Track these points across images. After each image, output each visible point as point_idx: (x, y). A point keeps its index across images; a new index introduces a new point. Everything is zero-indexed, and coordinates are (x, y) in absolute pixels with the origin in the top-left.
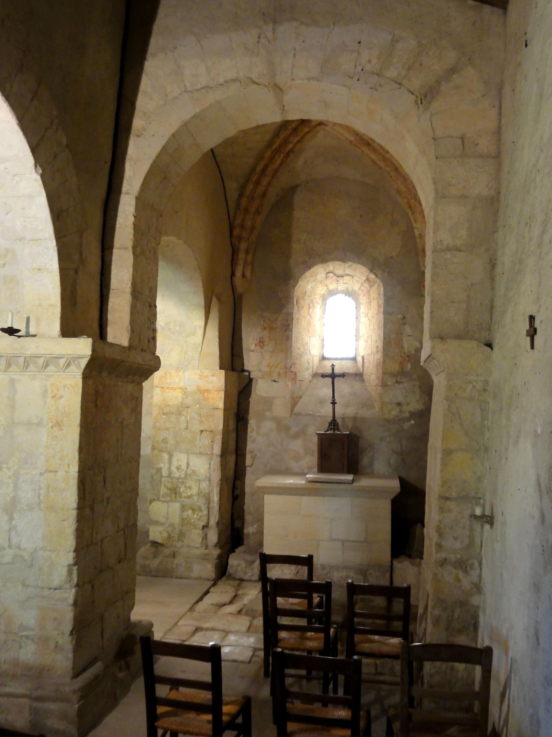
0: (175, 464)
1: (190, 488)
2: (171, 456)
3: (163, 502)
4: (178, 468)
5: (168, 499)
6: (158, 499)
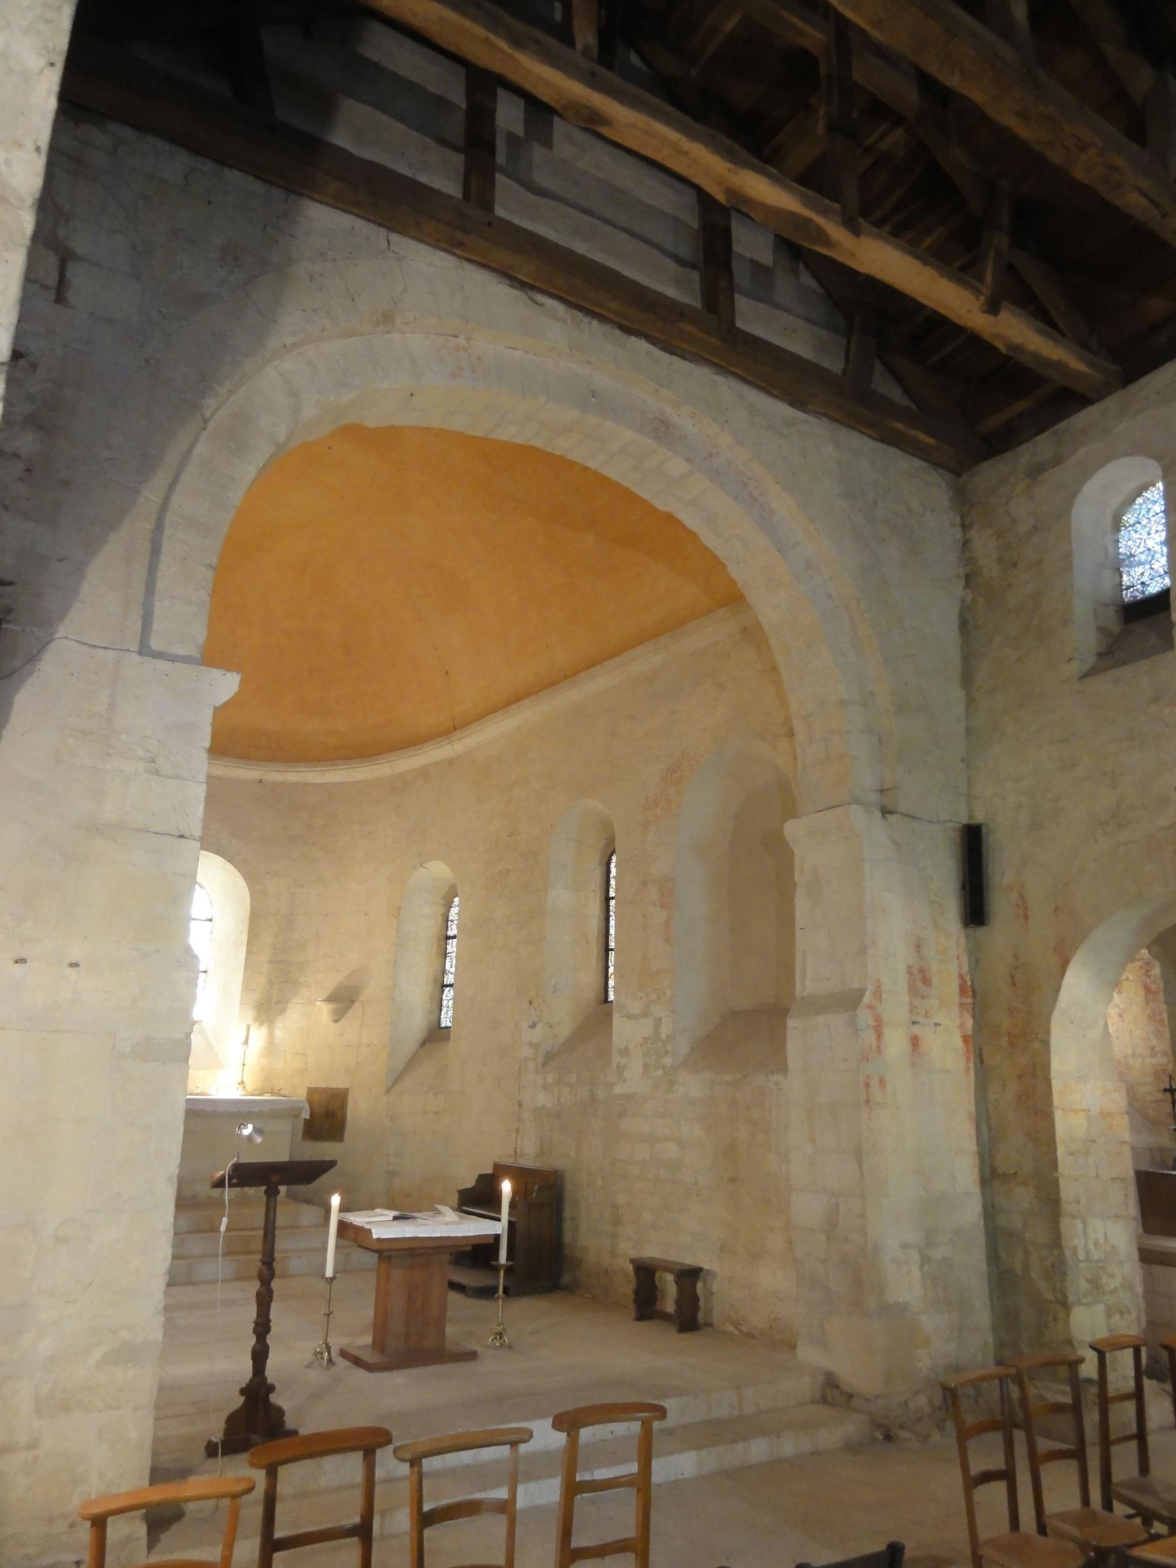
1: (1112, 1276)
2: (1085, 1224)
3: (1084, 1305)
4: (1096, 1244)
5: (1090, 1299)
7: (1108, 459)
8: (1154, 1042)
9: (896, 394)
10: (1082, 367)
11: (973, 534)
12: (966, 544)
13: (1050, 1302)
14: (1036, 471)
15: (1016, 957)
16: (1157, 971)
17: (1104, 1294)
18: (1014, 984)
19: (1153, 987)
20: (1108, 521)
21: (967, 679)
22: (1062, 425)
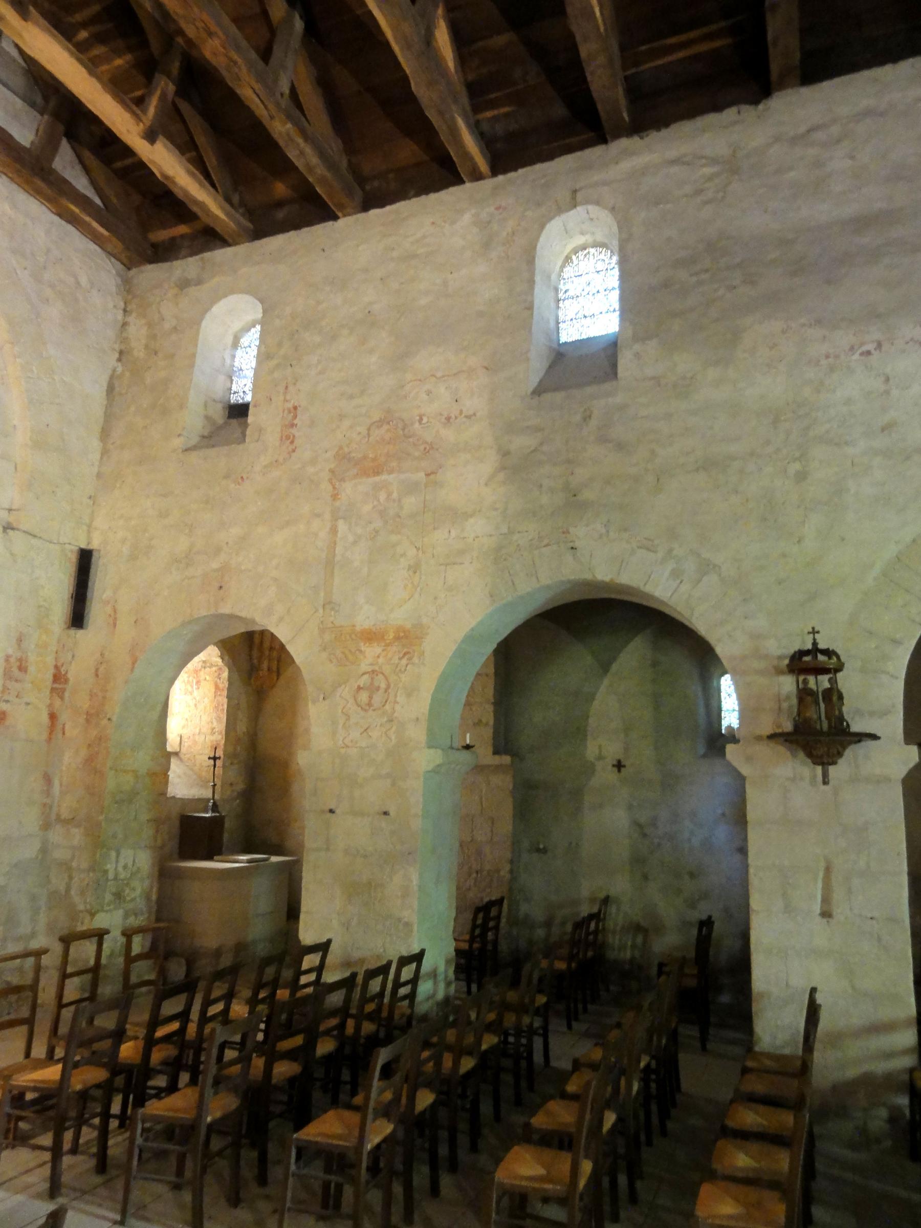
0: (122, 862)
1: (134, 889)
3: (107, 911)
6: (103, 911)
7: (232, 292)
8: (215, 724)
9: (82, 184)
10: (222, 216)
11: (131, 319)
12: (125, 324)
13: (81, 911)
14: (184, 284)
15: (102, 655)
16: (225, 674)
17: (124, 901)
18: (97, 675)
19: (221, 686)
20: (229, 340)
21: (105, 434)
22: (207, 255)
